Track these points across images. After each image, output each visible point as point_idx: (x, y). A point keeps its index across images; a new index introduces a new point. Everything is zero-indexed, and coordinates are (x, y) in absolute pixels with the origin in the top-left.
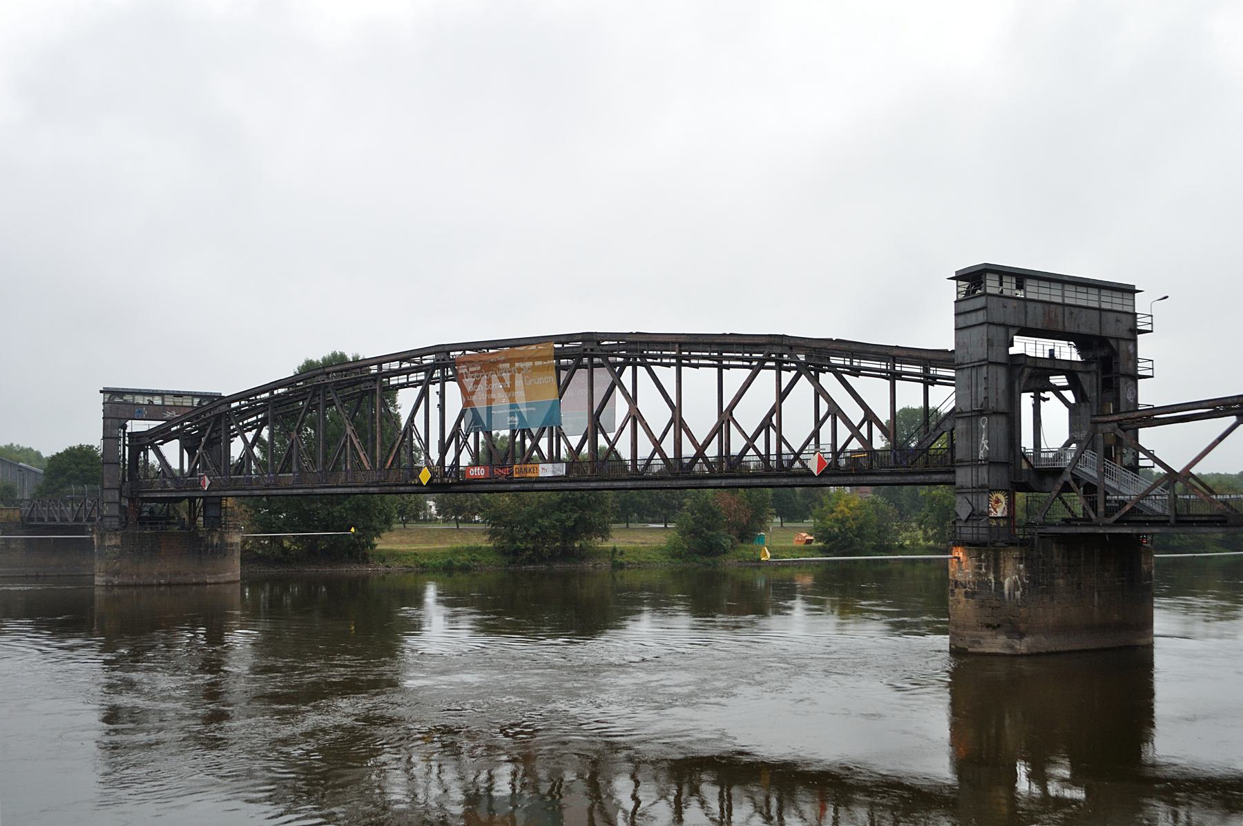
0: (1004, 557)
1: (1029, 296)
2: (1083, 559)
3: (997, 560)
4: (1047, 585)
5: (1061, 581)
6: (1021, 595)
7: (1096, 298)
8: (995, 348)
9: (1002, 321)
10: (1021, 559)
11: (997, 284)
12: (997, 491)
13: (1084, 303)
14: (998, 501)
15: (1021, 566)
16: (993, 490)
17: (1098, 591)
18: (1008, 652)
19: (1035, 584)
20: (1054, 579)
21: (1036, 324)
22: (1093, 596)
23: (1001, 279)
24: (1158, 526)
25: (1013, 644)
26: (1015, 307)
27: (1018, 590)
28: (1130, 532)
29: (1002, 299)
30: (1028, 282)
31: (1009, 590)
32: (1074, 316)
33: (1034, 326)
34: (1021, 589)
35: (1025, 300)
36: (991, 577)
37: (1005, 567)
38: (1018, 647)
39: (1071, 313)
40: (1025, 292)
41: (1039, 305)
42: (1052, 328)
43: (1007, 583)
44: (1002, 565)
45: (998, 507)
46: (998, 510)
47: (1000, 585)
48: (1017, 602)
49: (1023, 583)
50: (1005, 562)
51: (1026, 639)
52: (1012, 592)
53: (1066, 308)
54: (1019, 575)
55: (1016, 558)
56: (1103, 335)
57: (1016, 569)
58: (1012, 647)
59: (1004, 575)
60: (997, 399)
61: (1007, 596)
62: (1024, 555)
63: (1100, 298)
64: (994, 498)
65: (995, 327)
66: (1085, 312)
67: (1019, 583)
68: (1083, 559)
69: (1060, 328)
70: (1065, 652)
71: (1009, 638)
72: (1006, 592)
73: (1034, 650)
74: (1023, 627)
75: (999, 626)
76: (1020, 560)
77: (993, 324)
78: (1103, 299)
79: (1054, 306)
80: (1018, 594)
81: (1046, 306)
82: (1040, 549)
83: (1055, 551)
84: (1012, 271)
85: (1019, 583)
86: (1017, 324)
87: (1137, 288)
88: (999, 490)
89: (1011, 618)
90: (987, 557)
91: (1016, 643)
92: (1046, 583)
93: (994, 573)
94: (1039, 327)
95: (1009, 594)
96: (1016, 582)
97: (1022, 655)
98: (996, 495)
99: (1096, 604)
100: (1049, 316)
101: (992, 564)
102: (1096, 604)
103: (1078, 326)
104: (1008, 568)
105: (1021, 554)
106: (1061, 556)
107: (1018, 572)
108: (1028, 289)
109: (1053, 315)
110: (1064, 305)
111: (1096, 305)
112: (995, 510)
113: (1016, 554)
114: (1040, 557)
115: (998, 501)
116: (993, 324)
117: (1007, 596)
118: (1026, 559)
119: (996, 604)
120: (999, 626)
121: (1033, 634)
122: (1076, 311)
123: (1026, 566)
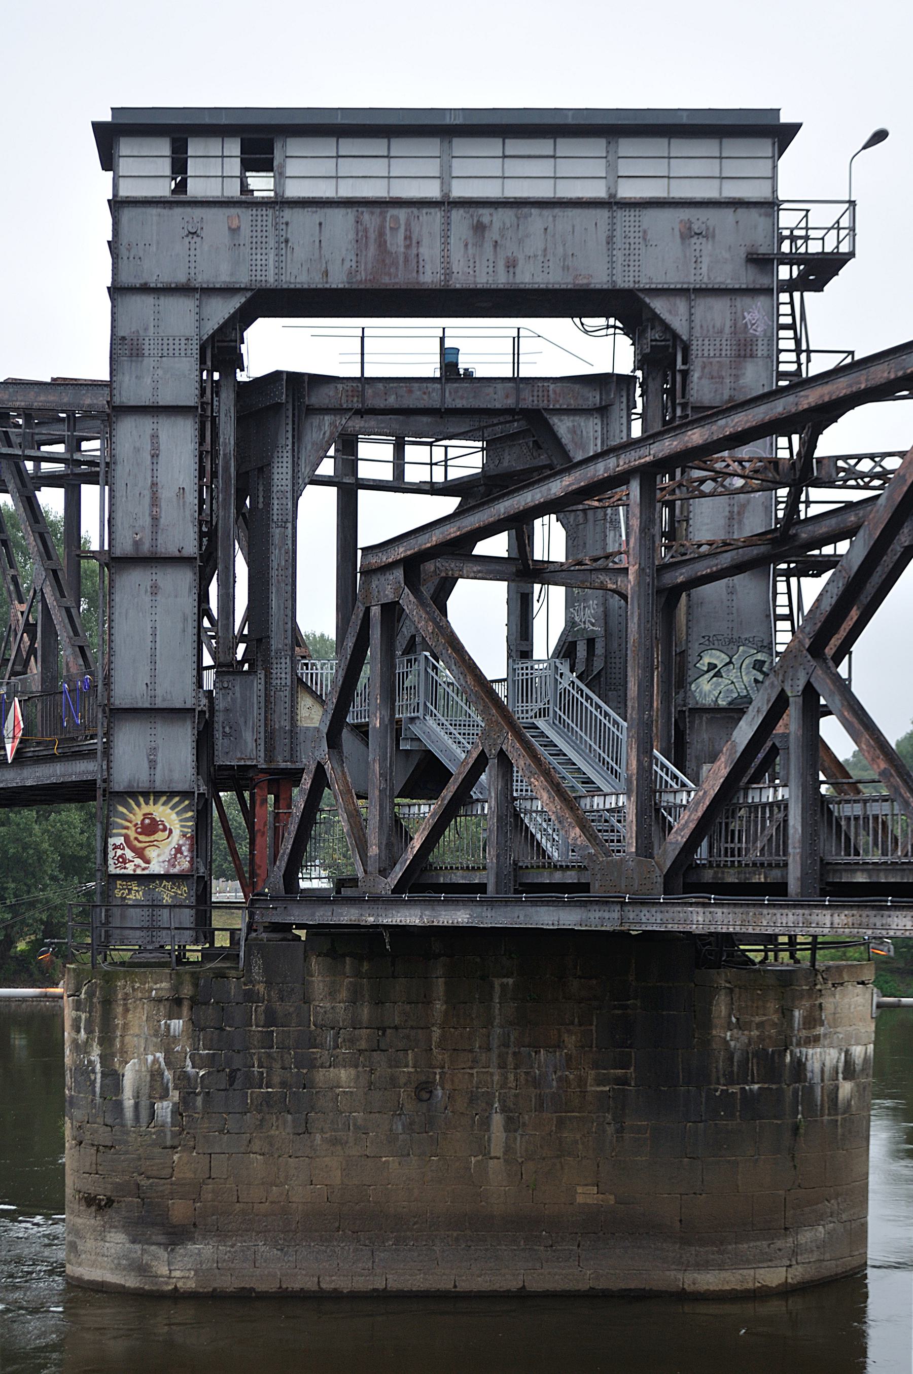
0: (126, 998)
1: (294, 190)
2: (439, 1006)
3: (107, 1003)
4: (283, 1084)
5: (344, 1075)
6: (177, 1112)
7: (598, 168)
8: (149, 362)
9: (181, 278)
10: (178, 1002)
11: (165, 167)
12: (152, 794)
13: (543, 191)
14: (151, 827)
15: (177, 1025)
16: (133, 794)
17: (504, 1109)
18: (131, 1282)
19: (232, 1078)
20: (312, 1065)
21: (326, 273)
22: (486, 1123)
24: (465, 903)
25: (146, 1258)
26: (234, 231)
27: (164, 1096)
28: (417, 922)
29: (189, 210)
30: (295, 146)
31: (137, 1096)
32: (493, 234)
33: (317, 282)
34: (175, 1095)
35: (279, 203)
36: (95, 1057)
37: (125, 1027)
38: (164, 1270)
39: (480, 228)
40: (280, 178)
41: (341, 220)
42: (399, 278)
43: (130, 1074)
44: (119, 1022)
45: (152, 844)
46: (151, 853)
47: (113, 1078)
48: (161, 1132)
49: (183, 1079)
50: (127, 1010)
51: (192, 1247)
52: (144, 1103)
53: (457, 215)
54: (168, 1053)
55: (159, 1000)
56: (621, 284)
57: (156, 1034)
58: (142, 1269)
59: (123, 1052)
60: (155, 519)
61: (129, 1113)
62: (187, 990)
63: (612, 167)
64: (138, 819)
65: (149, 300)
66: (537, 220)
67: (169, 1075)
68: (439, 1006)
69: (430, 277)
70: (355, 1296)
71: (133, 1242)
72: (129, 1102)
73: (228, 1283)
74: (179, 1210)
75: (110, 1202)
76: (174, 1004)
77: (145, 289)
78: (624, 168)
79: (402, 214)
80: (164, 1109)
81: (370, 218)
83: (319, 983)
84: (224, 121)
85: (169, 1075)
86: (243, 279)
87: (785, 118)
88: (158, 794)
89: (144, 1182)
90: (90, 994)
91: (156, 1258)
92: (276, 1080)
93: (101, 1044)
94: (338, 280)
95: (137, 1106)
96: (156, 1074)
97: (177, 1296)
98: (146, 809)
99: (497, 1149)
100: (382, 244)
101: (97, 1015)
102: (497, 1149)
103: (511, 264)
104: (135, 1030)
105: (176, 988)
106: (344, 994)
107: (167, 1042)
108: (293, 168)
109: (397, 243)
110: (447, 204)
111: (598, 191)
112: (140, 854)
113: (162, 986)
114: (250, 997)
115: (151, 827)
116: (145, 289)
117: (129, 1113)
118: (195, 1002)
119: (103, 1136)
120: (110, 1202)
121: (221, 1234)
122: (500, 218)
123: (196, 1026)
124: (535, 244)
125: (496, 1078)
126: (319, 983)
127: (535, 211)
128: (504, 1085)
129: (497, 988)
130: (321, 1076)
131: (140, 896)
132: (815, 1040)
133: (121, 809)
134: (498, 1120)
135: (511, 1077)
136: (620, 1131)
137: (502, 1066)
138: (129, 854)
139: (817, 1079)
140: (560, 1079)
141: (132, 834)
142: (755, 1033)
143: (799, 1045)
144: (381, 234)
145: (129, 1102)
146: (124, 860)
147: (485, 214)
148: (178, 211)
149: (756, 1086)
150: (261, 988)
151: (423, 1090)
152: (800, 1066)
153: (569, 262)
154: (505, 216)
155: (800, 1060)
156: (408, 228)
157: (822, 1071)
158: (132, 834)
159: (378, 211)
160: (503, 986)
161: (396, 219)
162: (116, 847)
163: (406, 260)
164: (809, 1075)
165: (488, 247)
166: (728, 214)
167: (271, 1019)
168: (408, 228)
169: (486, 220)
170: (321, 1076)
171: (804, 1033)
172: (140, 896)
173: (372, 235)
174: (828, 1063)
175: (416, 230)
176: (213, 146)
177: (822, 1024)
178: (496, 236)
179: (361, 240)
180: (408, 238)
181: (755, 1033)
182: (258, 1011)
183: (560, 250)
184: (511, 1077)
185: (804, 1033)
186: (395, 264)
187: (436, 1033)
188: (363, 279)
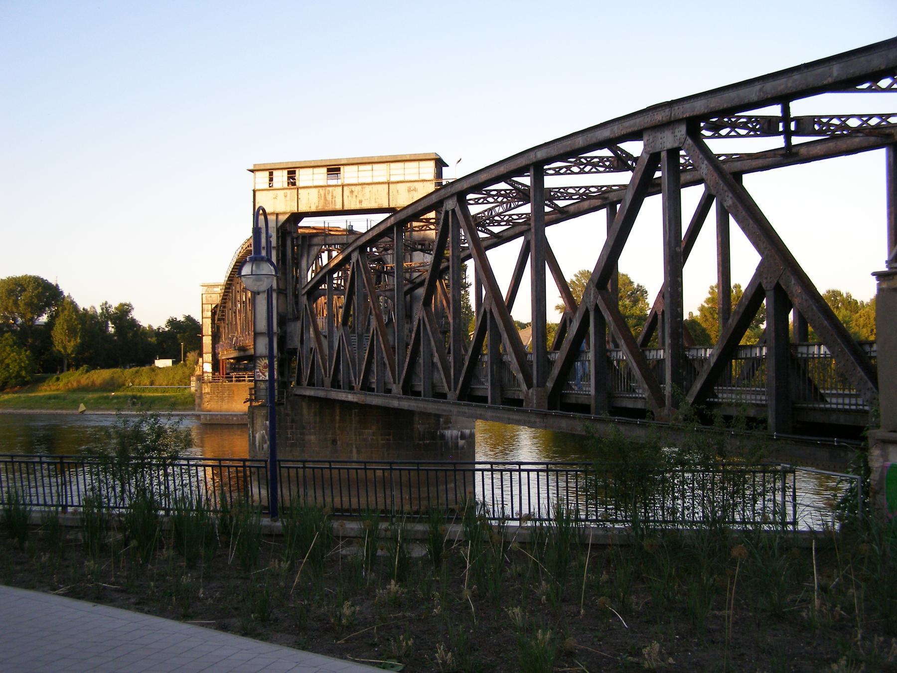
2: (338, 418)
5: (313, 437)
17: (356, 448)
21: (310, 207)
23: (271, 174)
26: (286, 196)
27: (266, 443)
31: (259, 443)
32: (355, 193)
39: (352, 192)
41: (315, 191)
43: (257, 436)
52: (261, 446)
57: (263, 425)
59: (256, 430)
61: (257, 447)
66: (368, 188)
68: (338, 418)
72: (257, 445)
79: (330, 189)
80: (266, 446)
81: (322, 191)
82: (289, 407)
83: (305, 411)
94: (313, 209)
95: (259, 446)
96: (263, 437)
103: (361, 202)
106: (312, 414)
109: (329, 198)
114: (287, 415)
117: (257, 447)
122: (356, 189)
124: (367, 195)
125: (354, 438)
126: (305, 411)
127: (367, 186)
128: (356, 440)
129: (353, 413)
130: (307, 437)
131: (264, 386)
132: (449, 428)
133: (258, 361)
134: (354, 450)
135: (358, 438)
136: (388, 454)
137: (355, 435)
138: (261, 374)
139: (450, 439)
140: (372, 439)
141: (261, 368)
142: (427, 426)
143: (442, 429)
144: (325, 195)
145: (257, 445)
146: (260, 376)
147: (353, 188)
148: (271, 192)
149: (428, 442)
150: (290, 412)
151: (334, 442)
152: (443, 436)
153: (377, 200)
154: (359, 188)
155: (443, 434)
156: (332, 192)
157: (452, 438)
158: (261, 368)
159: (324, 188)
160: (355, 412)
161: (329, 191)
162: (257, 372)
163: (332, 202)
164: (446, 438)
165: (354, 197)
166: (421, 184)
167: (293, 421)
168: (332, 192)
169: (353, 190)
170: (307, 437)
171: (444, 426)
172: (264, 386)
173: (323, 195)
174: (454, 435)
175: (334, 192)
176: (280, 172)
177: (451, 423)
178: (356, 194)
179: (319, 197)
180: (332, 196)
181: (427, 426)
182: (289, 419)
183: (374, 197)
184: (358, 438)
185: (444, 426)
186: (329, 203)
187: (337, 425)
188: (320, 209)
